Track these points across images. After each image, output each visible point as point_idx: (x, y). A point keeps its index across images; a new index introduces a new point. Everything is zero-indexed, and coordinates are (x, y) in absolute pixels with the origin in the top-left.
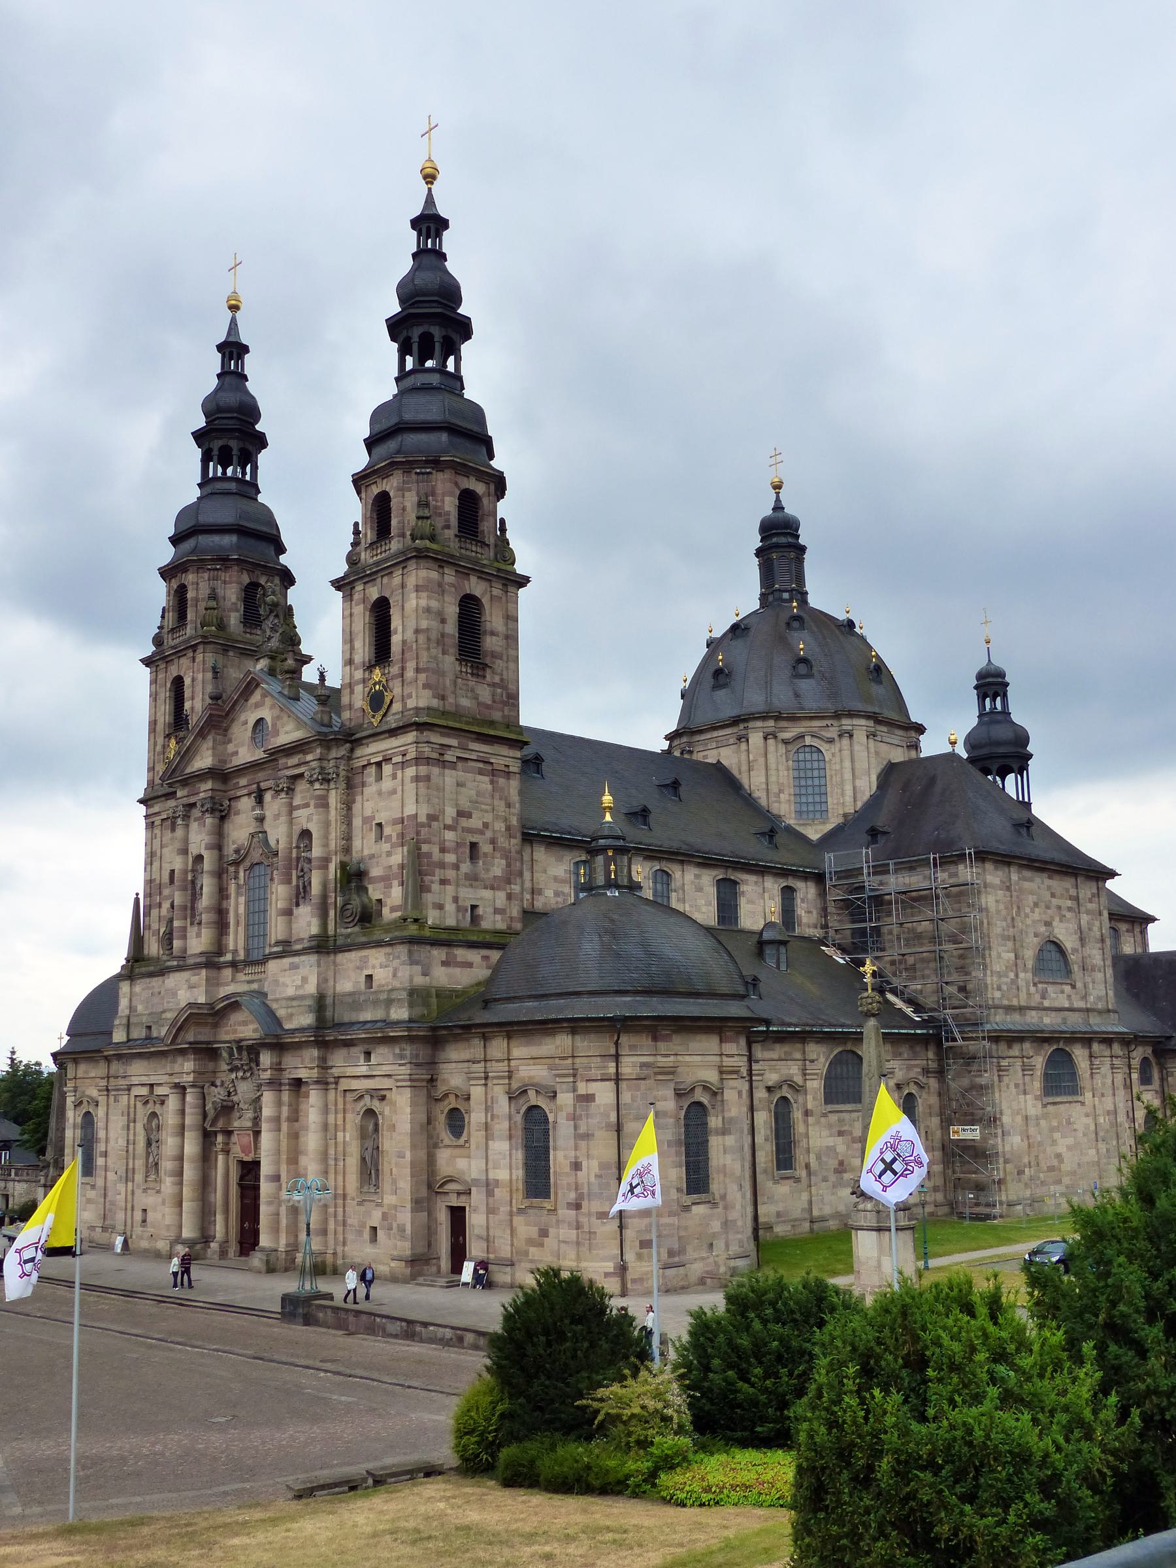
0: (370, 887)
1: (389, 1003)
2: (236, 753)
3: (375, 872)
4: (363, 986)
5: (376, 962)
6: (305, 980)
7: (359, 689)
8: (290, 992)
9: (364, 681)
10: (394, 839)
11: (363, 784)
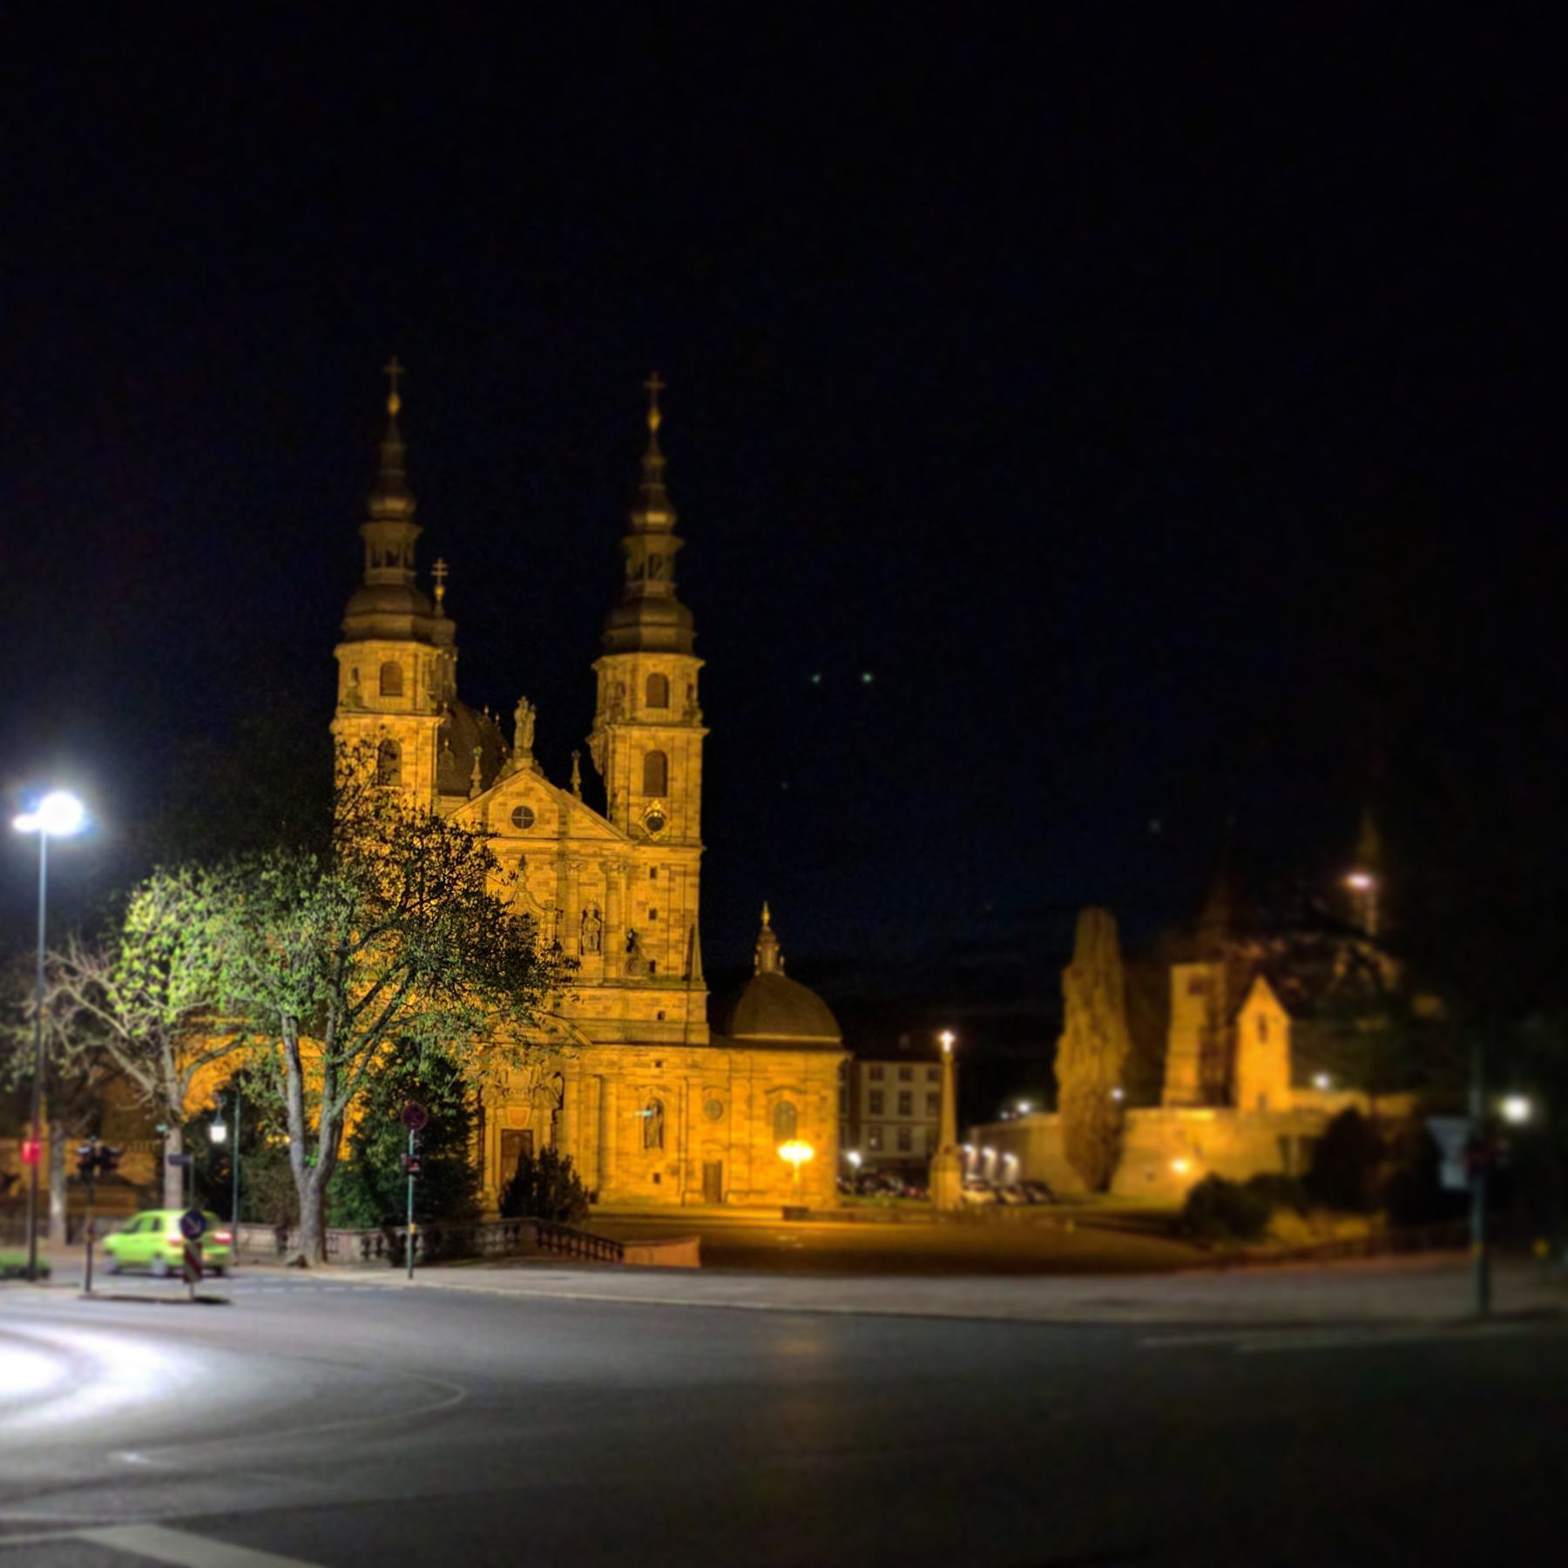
0: (644, 951)
1: (686, 1031)
2: (493, 826)
3: (647, 941)
4: (655, 1017)
5: (671, 1004)
6: (607, 1009)
7: (634, 811)
8: (591, 1014)
9: (639, 805)
10: (672, 922)
11: (638, 879)
